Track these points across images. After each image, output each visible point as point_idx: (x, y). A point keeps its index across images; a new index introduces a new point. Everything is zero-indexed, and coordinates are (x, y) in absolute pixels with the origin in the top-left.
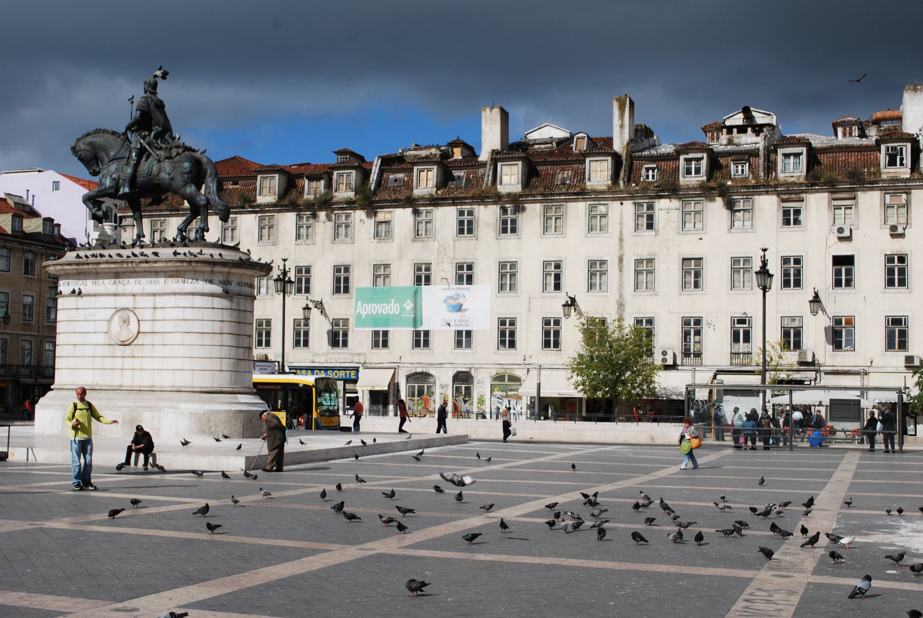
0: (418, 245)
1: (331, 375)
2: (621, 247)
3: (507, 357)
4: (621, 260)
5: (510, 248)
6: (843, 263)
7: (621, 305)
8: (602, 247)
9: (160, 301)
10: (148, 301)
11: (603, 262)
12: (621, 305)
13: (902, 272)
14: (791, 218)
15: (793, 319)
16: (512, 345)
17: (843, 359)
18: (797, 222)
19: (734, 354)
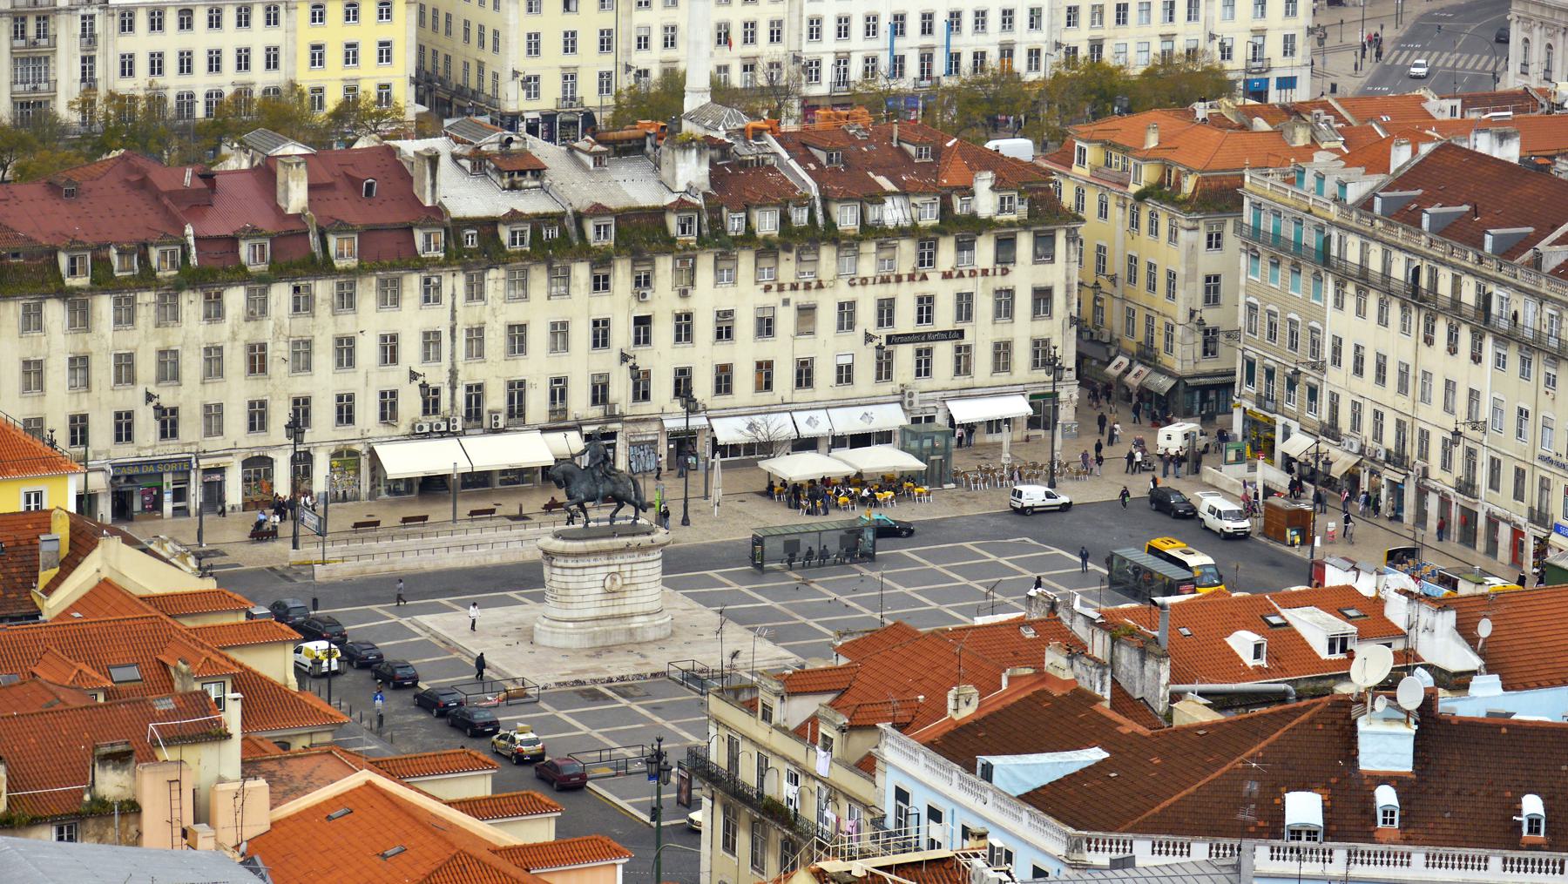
0: (252, 324)
1: (160, 469)
2: (453, 318)
3: (346, 433)
4: (453, 330)
5: (347, 324)
6: (643, 323)
7: (453, 373)
8: (437, 318)
9: (635, 567)
10: (628, 568)
11: (437, 334)
12: (453, 373)
13: (688, 328)
14: (601, 284)
15: (600, 376)
16: (350, 420)
17: (644, 409)
18: (606, 287)
19: (552, 412)
